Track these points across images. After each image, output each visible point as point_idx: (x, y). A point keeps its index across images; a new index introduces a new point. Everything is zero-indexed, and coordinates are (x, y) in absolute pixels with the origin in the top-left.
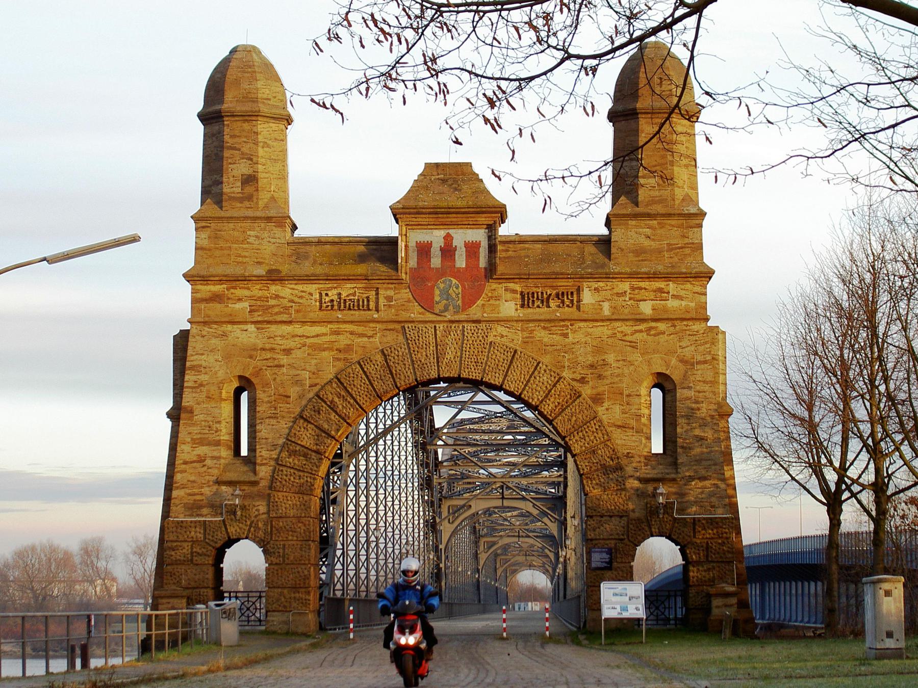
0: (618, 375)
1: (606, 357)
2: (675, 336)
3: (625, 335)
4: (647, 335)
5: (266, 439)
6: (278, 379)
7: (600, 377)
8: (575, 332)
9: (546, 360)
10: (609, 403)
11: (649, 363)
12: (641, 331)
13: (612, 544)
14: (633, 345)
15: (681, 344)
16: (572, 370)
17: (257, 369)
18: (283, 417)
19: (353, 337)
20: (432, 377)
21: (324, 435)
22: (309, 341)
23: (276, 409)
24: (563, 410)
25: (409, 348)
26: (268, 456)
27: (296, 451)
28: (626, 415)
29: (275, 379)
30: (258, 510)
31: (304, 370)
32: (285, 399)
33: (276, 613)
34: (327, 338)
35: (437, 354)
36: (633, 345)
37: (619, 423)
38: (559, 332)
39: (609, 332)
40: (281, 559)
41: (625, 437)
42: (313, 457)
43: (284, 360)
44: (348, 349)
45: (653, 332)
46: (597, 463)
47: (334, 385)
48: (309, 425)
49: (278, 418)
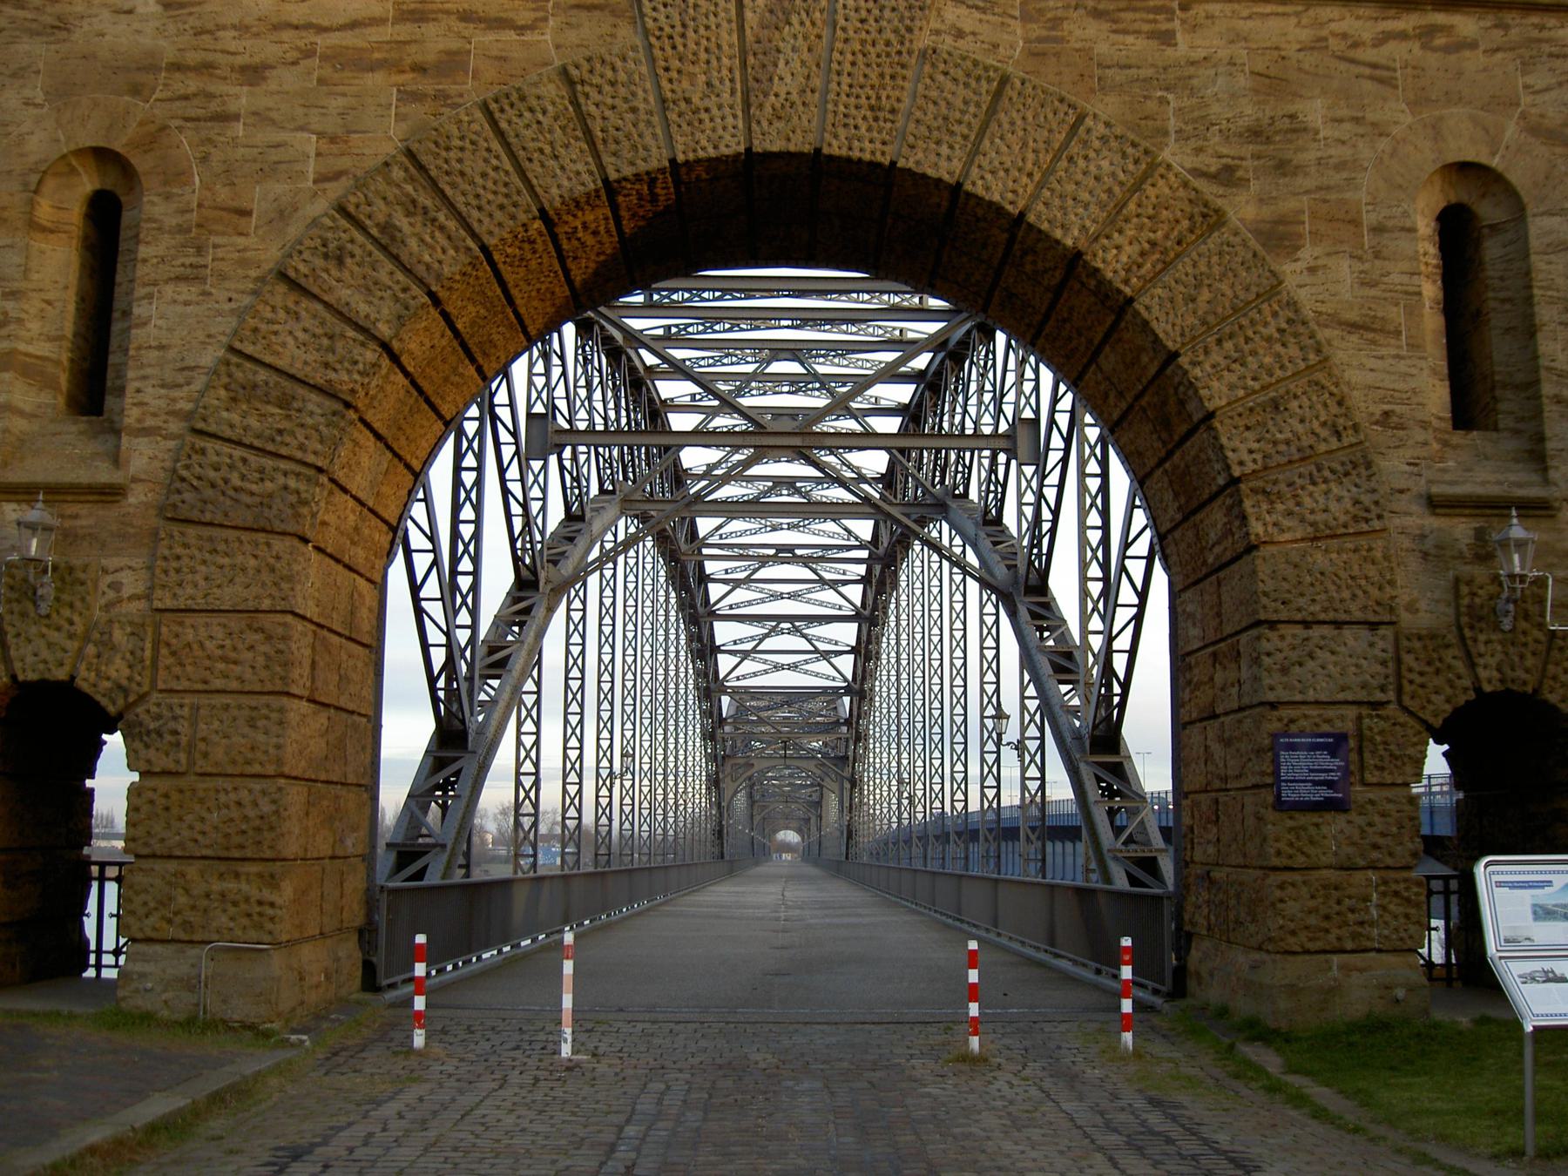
0: (1341, 166)
1: (1296, 107)
2: (1510, 55)
3: (1355, 45)
4: (1424, 47)
5: (161, 347)
6: (217, 156)
7: (1283, 167)
8: (1194, 28)
9: (1106, 108)
10: (1318, 251)
11: (1436, 130)
12: (1403, 36)
13: (1345, 719)
14: (1382, 76)
15: (1529, 80)
16: (1193, 143)
17: (152, 128)
18: (223, 277)
19: (468, 29)
20: (726, 151)
21: (351, 333)
22: (323, 42)
23: (200, 251)
24: (1167, 265)
25: (652, 60)
26: (162, 403)
27: (255, 386)
28: (1373, 292)
29: (205, 159)
30: (116, 586)
31: (302, 129)
32: (235, 218)
33: (158, 948)
34: (387, 33)
35: (744, 81)
36: (1382, 76)
37: (1352, 316)
38: (1146, 27)
39: (1305, 35)
40: (183, 757)
41: (1371, 363)
42: (310, 407)
43: (242, 99)
44: (452, 63)
45: (1440, 41)
46: (1288, 442)
47: (397, 174)
48: (305, 303)
49: (203, 280)
